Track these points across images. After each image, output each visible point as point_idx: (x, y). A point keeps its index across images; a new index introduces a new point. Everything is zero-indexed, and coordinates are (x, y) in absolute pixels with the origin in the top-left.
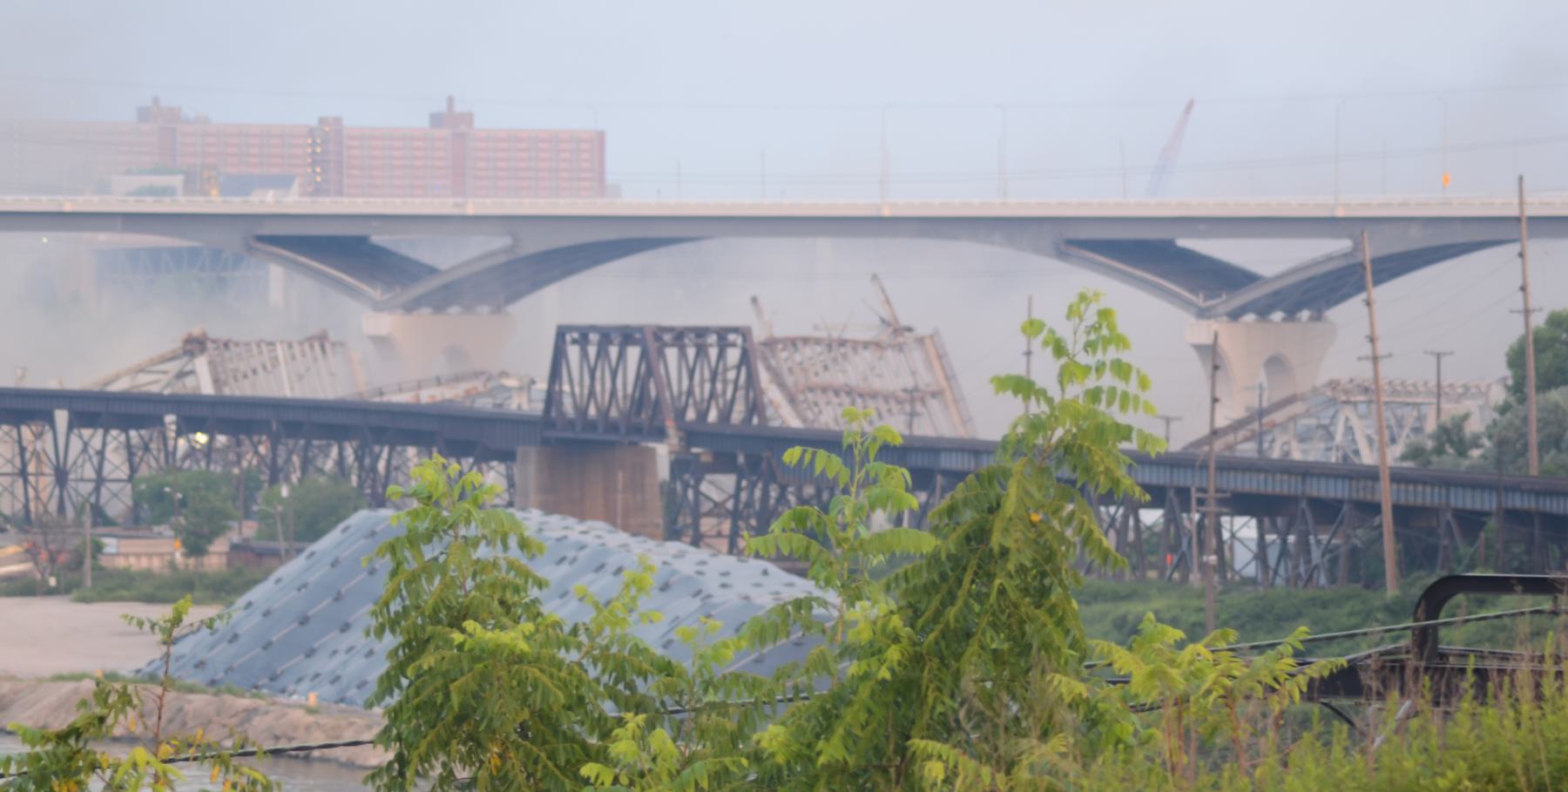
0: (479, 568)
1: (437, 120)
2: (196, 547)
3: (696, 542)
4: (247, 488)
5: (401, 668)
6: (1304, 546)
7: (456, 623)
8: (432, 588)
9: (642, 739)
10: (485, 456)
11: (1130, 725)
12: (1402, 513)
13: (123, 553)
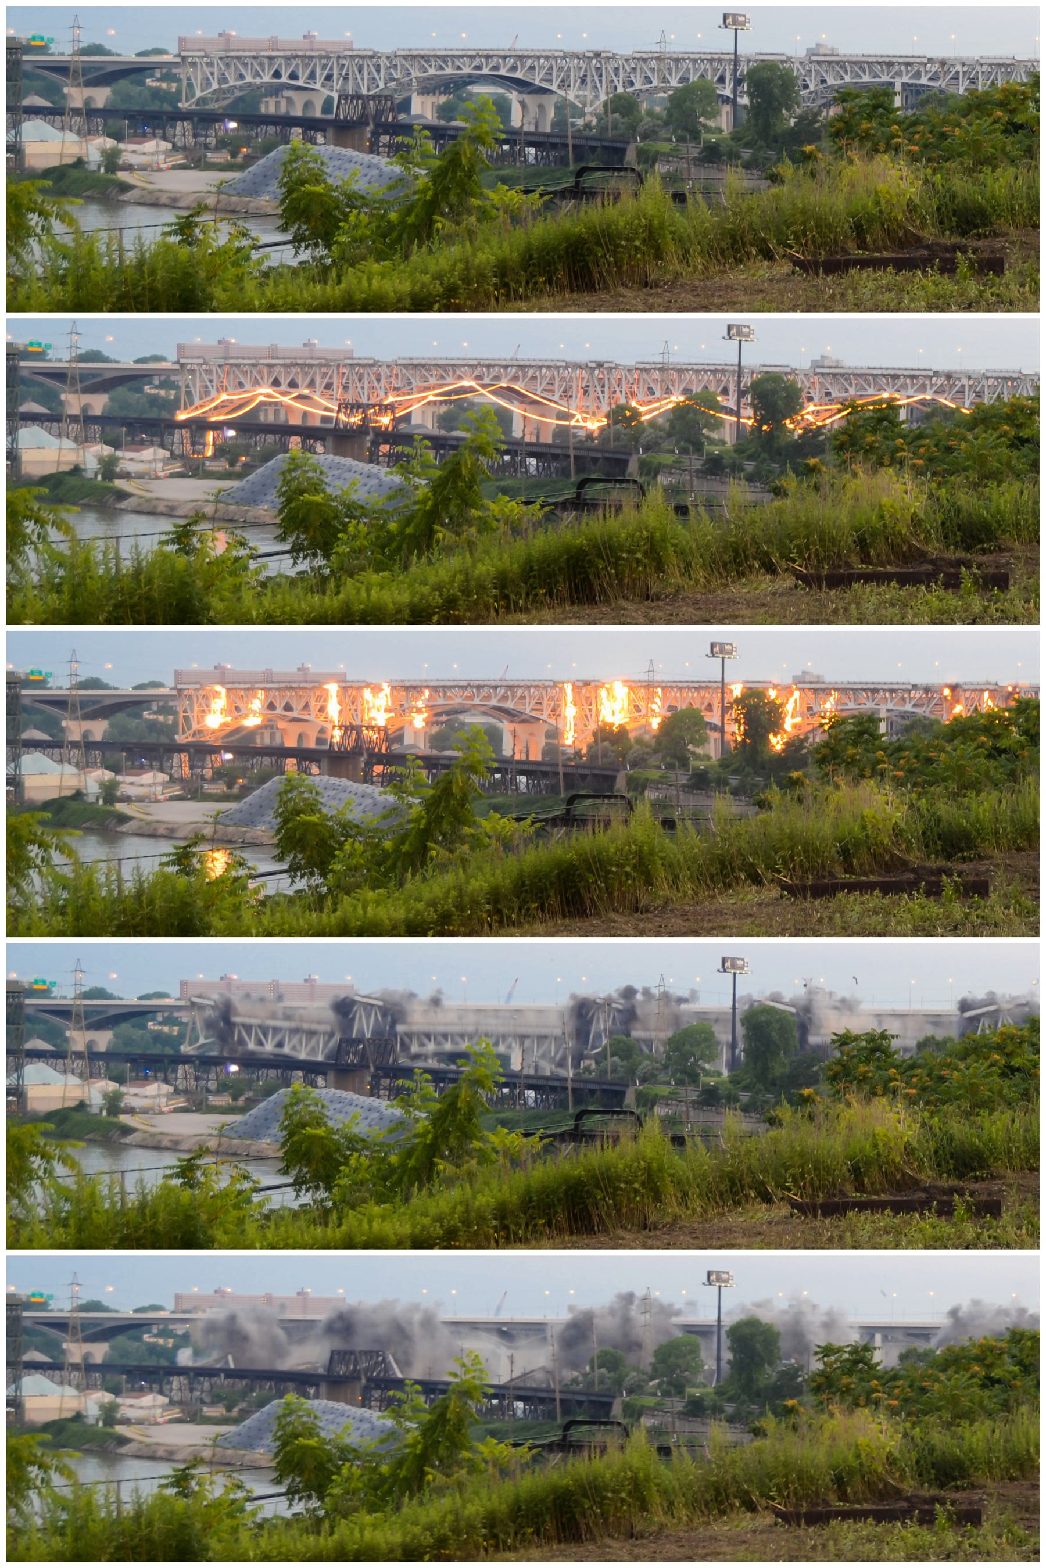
0: (309, 479)
1: (305, 345)
2: (232, 464)
3: (378, 464)
4: (248, 447)
5: (284, 507)
6: (549, 467)
7: (301, 494)
8: (294, 485)
9: (356, 528)
10: (316, 439)
11: (495, 524)
12: (576, 457)
13: (211, 466)
